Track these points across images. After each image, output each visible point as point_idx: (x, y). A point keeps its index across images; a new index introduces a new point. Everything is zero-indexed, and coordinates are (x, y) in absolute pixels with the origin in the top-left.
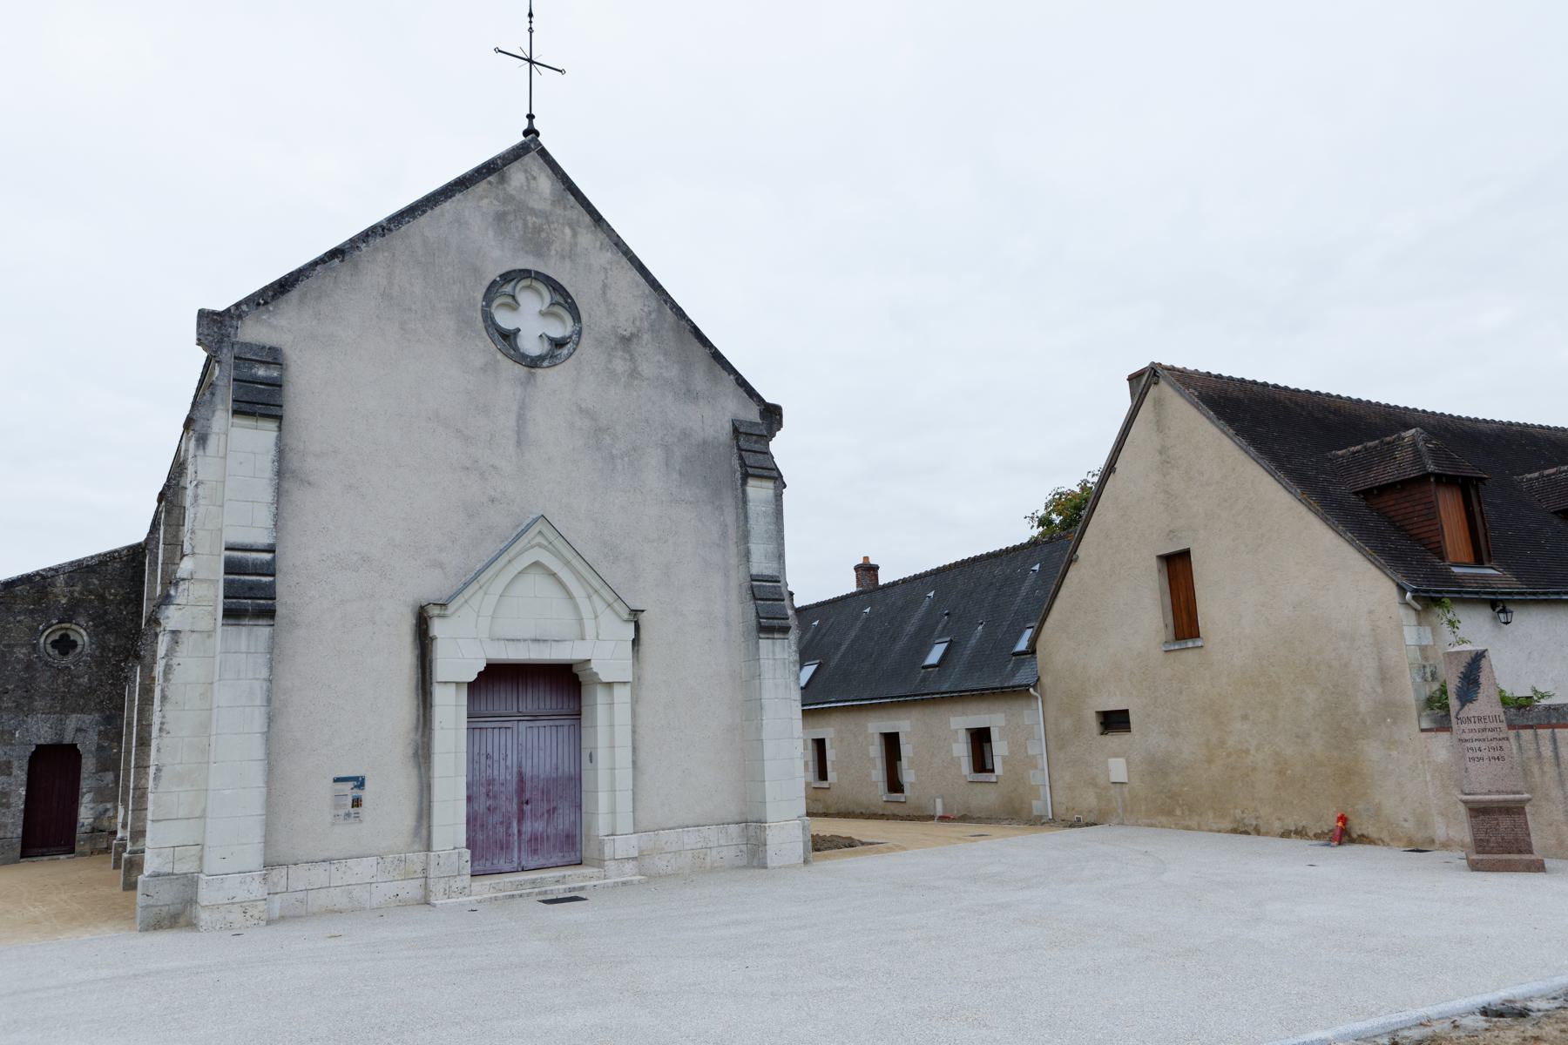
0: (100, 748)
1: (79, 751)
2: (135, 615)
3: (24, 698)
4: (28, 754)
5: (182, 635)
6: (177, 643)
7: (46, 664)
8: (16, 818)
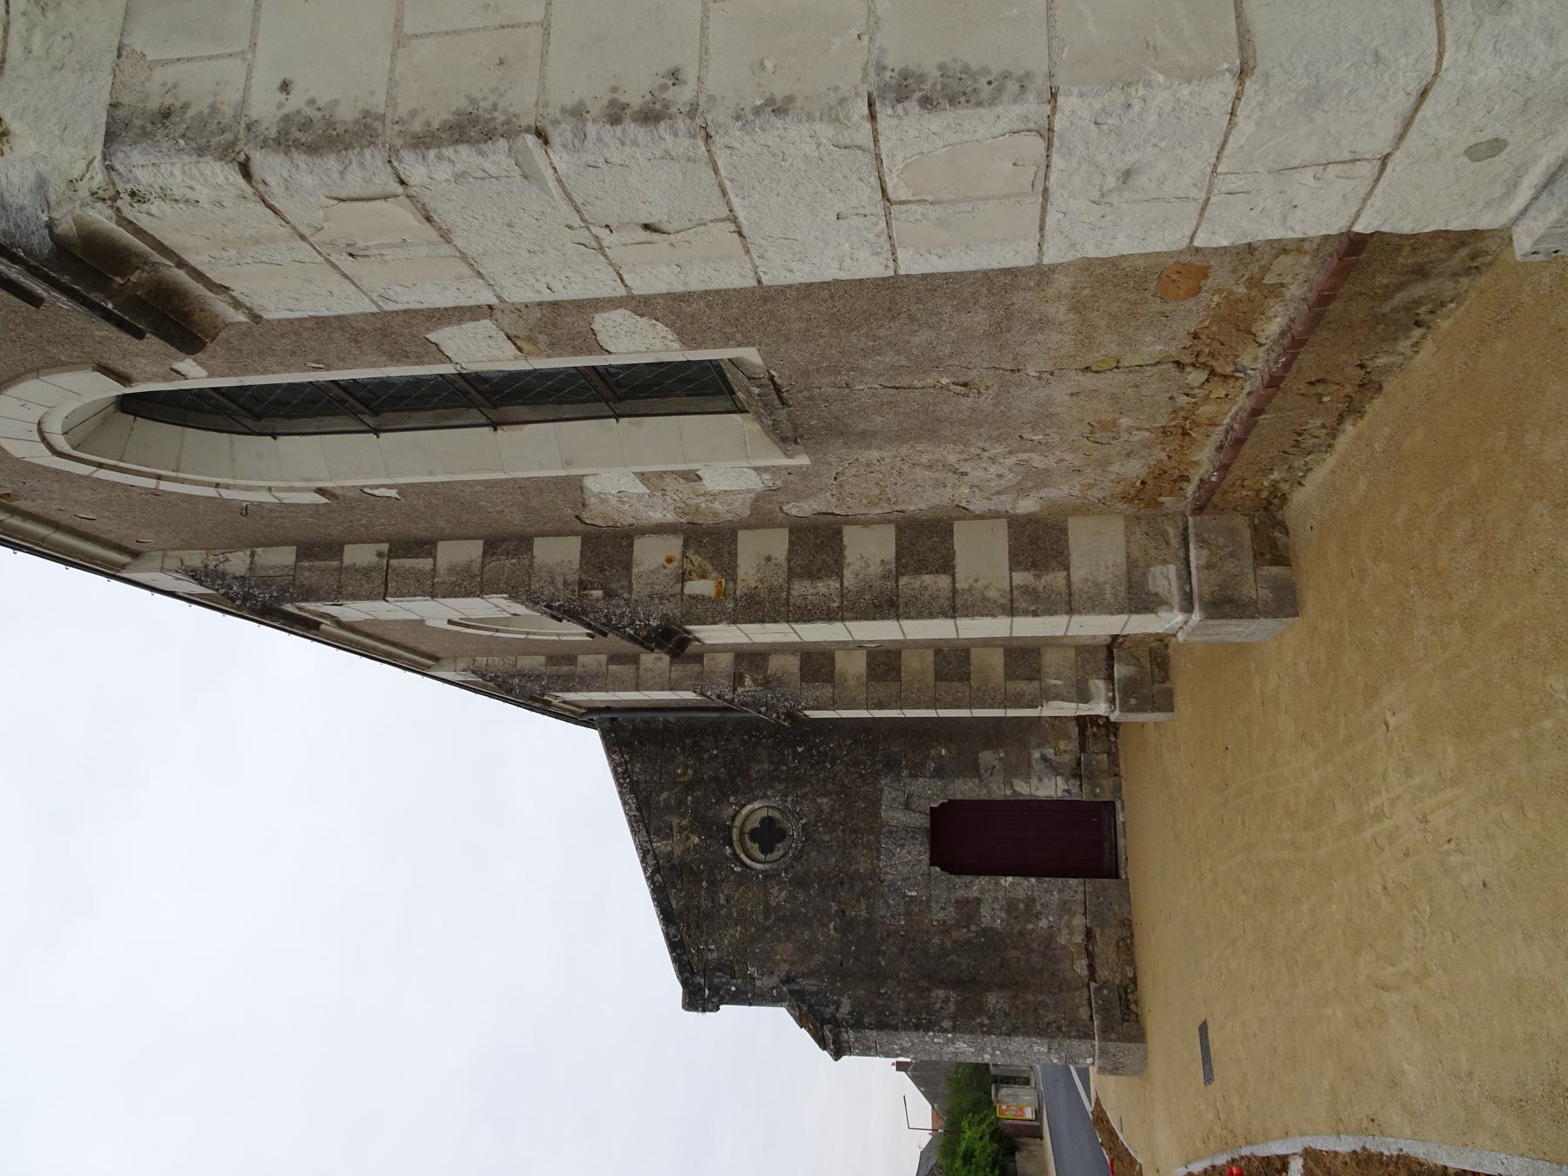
0: (939, 773)
4: (945, 876)
5: (127, 98)
6: (166, 114)
7: (797, 858)
8: (1052, 888)
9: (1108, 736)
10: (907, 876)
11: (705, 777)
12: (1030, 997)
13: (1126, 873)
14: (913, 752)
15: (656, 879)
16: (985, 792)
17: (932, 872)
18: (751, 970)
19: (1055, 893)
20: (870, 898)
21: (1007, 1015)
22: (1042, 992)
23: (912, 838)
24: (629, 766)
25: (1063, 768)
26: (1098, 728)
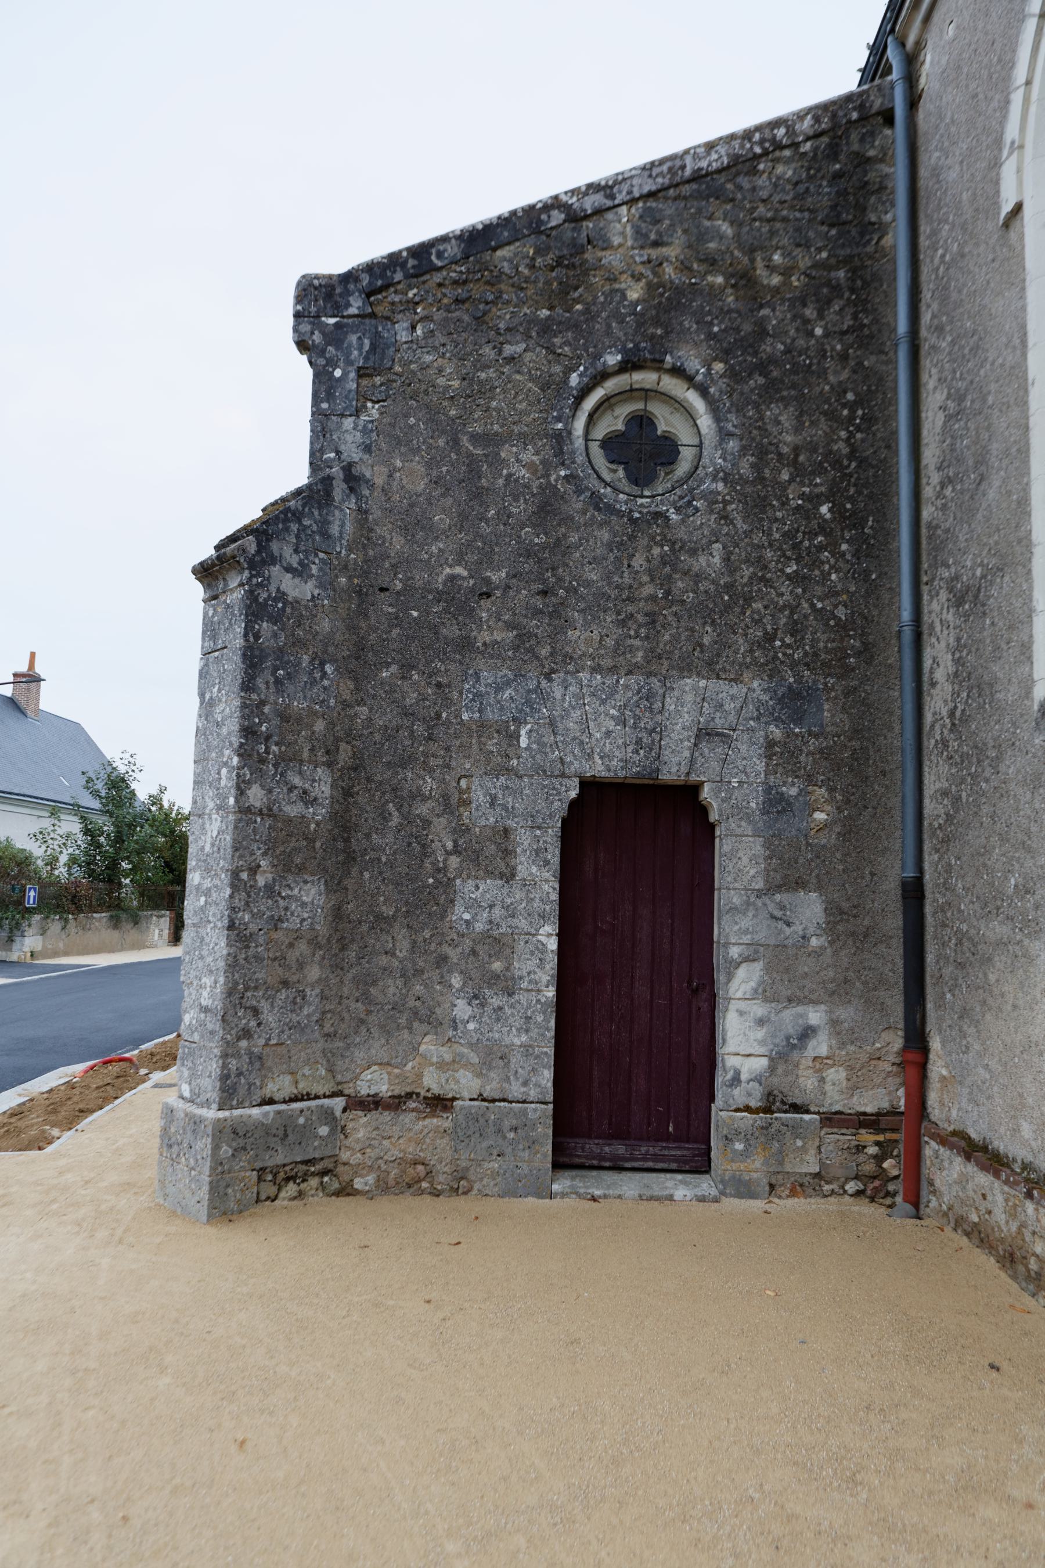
1: (703, 810)
2: (850, 338)
3: (537, 612)
4: (560, 809)
7: (595, 500)
8: (534, 1034)
9: (857, 1177)
10: (561, 726)
11: (765, 312)
12: (314, 973)
13: (563, 1195)
14: (821, 751)
15: (555, 213)
16: (736, 901)
17: (565, 781)
18: (373, 410)
19: (524, 1038)
20: (516, 648)
21: (276, 923)
22: (323, 997)
24: (787, 153)
26: (875, 1157)
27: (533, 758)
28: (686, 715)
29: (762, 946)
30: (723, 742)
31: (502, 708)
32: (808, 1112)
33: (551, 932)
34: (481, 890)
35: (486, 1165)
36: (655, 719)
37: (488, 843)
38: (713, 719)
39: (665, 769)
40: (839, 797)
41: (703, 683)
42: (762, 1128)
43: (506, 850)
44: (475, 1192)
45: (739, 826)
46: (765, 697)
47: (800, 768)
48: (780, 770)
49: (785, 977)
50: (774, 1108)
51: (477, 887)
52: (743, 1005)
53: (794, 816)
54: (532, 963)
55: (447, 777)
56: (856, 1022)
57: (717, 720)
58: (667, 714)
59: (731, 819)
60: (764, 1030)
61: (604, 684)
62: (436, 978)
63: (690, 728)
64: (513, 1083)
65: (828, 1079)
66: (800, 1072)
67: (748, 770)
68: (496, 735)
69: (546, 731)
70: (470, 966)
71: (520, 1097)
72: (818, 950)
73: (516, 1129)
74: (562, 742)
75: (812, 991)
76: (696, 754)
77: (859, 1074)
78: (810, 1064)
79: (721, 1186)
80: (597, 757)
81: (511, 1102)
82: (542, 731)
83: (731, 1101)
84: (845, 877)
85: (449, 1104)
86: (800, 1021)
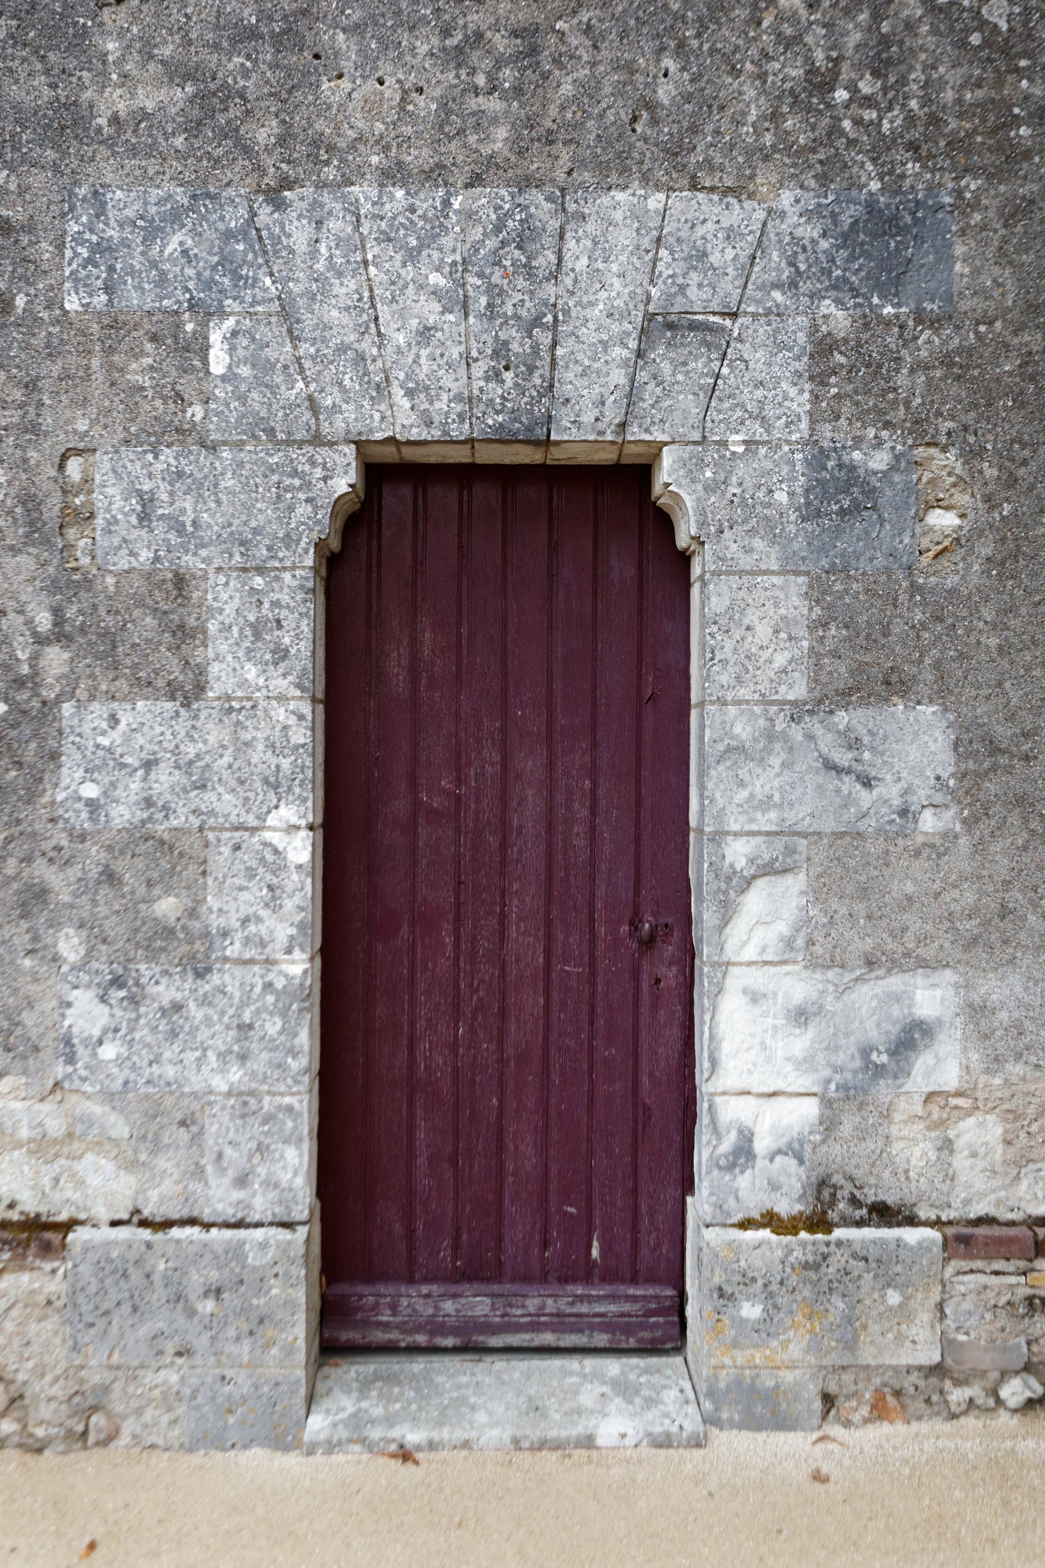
8: (260, 1061)
9: (1028, 1368)
10: (308, 321)
13: (331, 1447)
14: (947, 360)
16: (742, 730)
17: (323, 454)
19: (236, 1075)
20: (193, 129)
23: (500, 351)
25: (862, 1134)
27: (242, 399)
28: (617, 282)
29: (804, 835)
30: (708, 345)
31: (162, 280)
32: (912, 1221)
33: (294, 820)
34: (122, 726)
35: (149, 1378)
36: (540, 294)
37: (137, 613)
38: (683, 288)
39: (564, 417)
40: (991, 472)
41: (656, 201)
42: (806, 1266)
43: (182, 627)
44: (124, 1439)
45: (748, 550)
46: (809, 231)
47: (895, 401)
48: (847, 408)
49: (860, 909)
50: (833, 1215)
51: (114, 720)
52: (757, 978)
53: (882, 520)
54: (252, 898)
55: (33, 455)
56: (1028, 1007)
57: (693, 293)
58: (569, 281)
59: (727, 534)
60: (811, 1033)
61: (412, 210)
62: (23, 940)
63: (625, 314)
64: (213, 1181)
65: (960, 1144)
66: (894, 1130)
67: (770, 412)
68: (149, 347)
69: (272, 332)
70: (102, 910)
71: (230, 1213)
72: (938, 841)
73: (218, 1291)
74: (313, 358)
75: (923, 940)
76: (643, 376)
77: (1034, 1128)
78: (919, 1109)
79: (708, 1405)
80: (398, 393)
81: (208, 1226)
82: (263, 333)
83: (732, 1202)
84: (1005, 663)
85: (53, 1237)
86: (896, 1011)
